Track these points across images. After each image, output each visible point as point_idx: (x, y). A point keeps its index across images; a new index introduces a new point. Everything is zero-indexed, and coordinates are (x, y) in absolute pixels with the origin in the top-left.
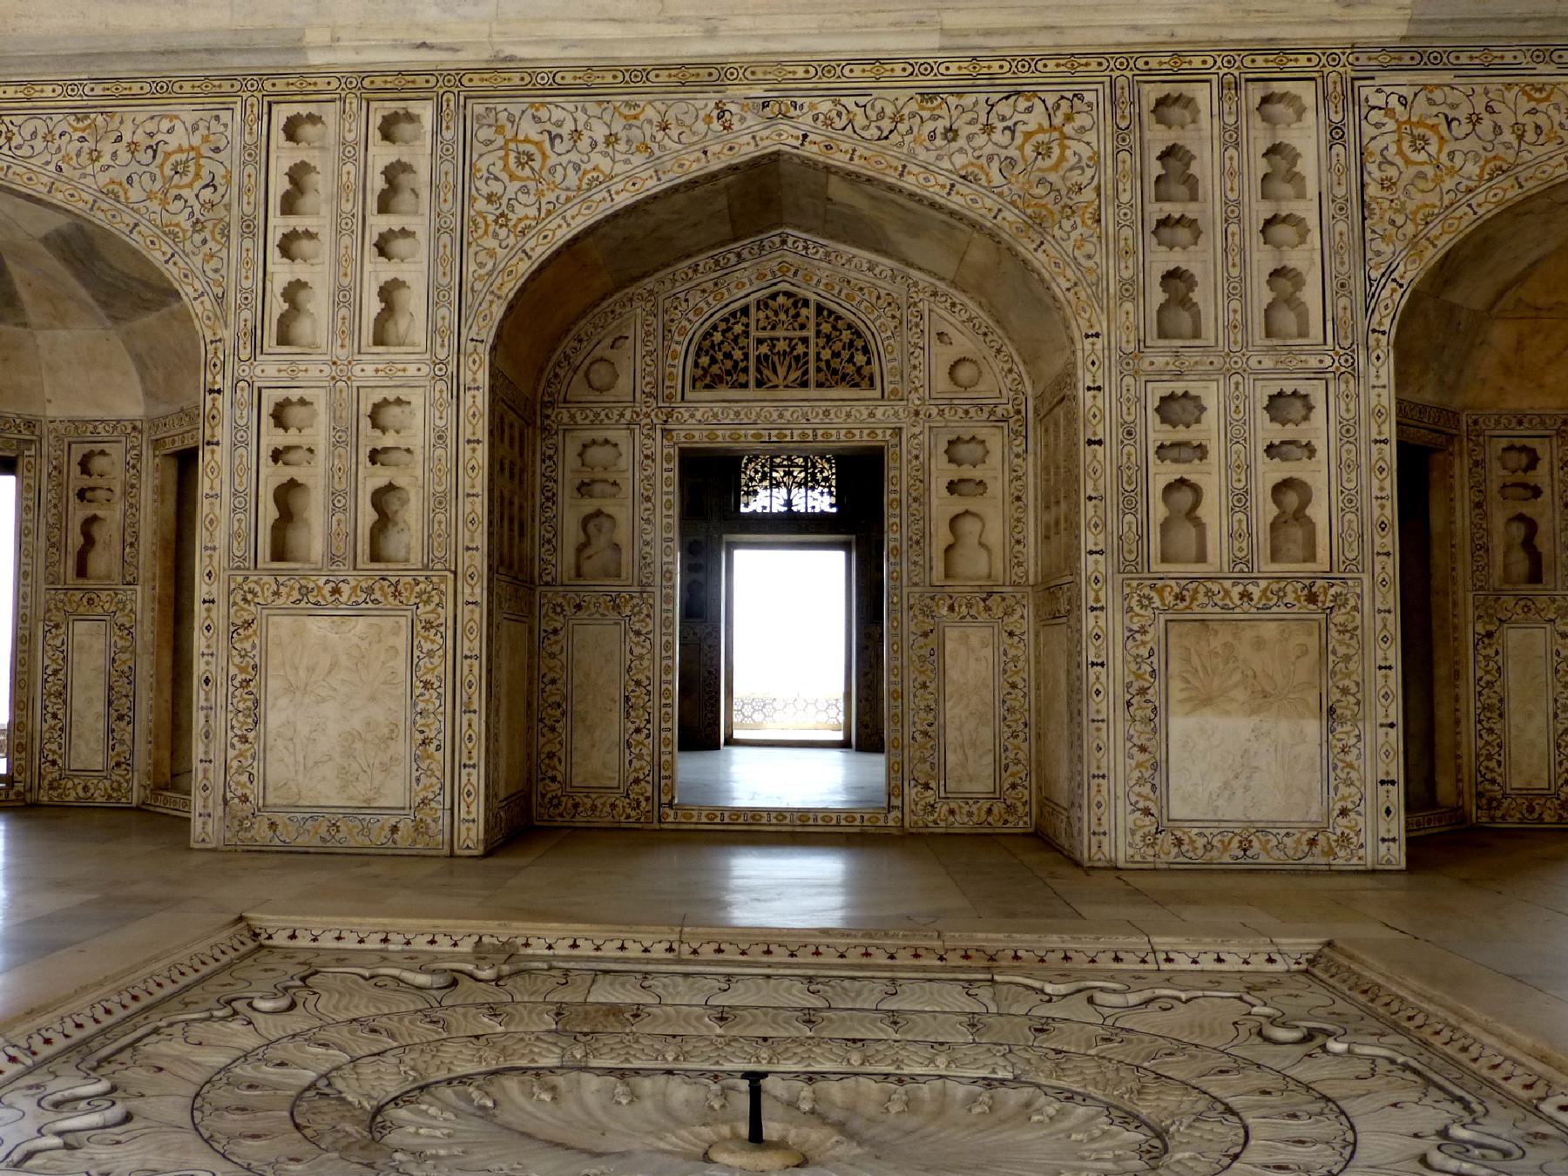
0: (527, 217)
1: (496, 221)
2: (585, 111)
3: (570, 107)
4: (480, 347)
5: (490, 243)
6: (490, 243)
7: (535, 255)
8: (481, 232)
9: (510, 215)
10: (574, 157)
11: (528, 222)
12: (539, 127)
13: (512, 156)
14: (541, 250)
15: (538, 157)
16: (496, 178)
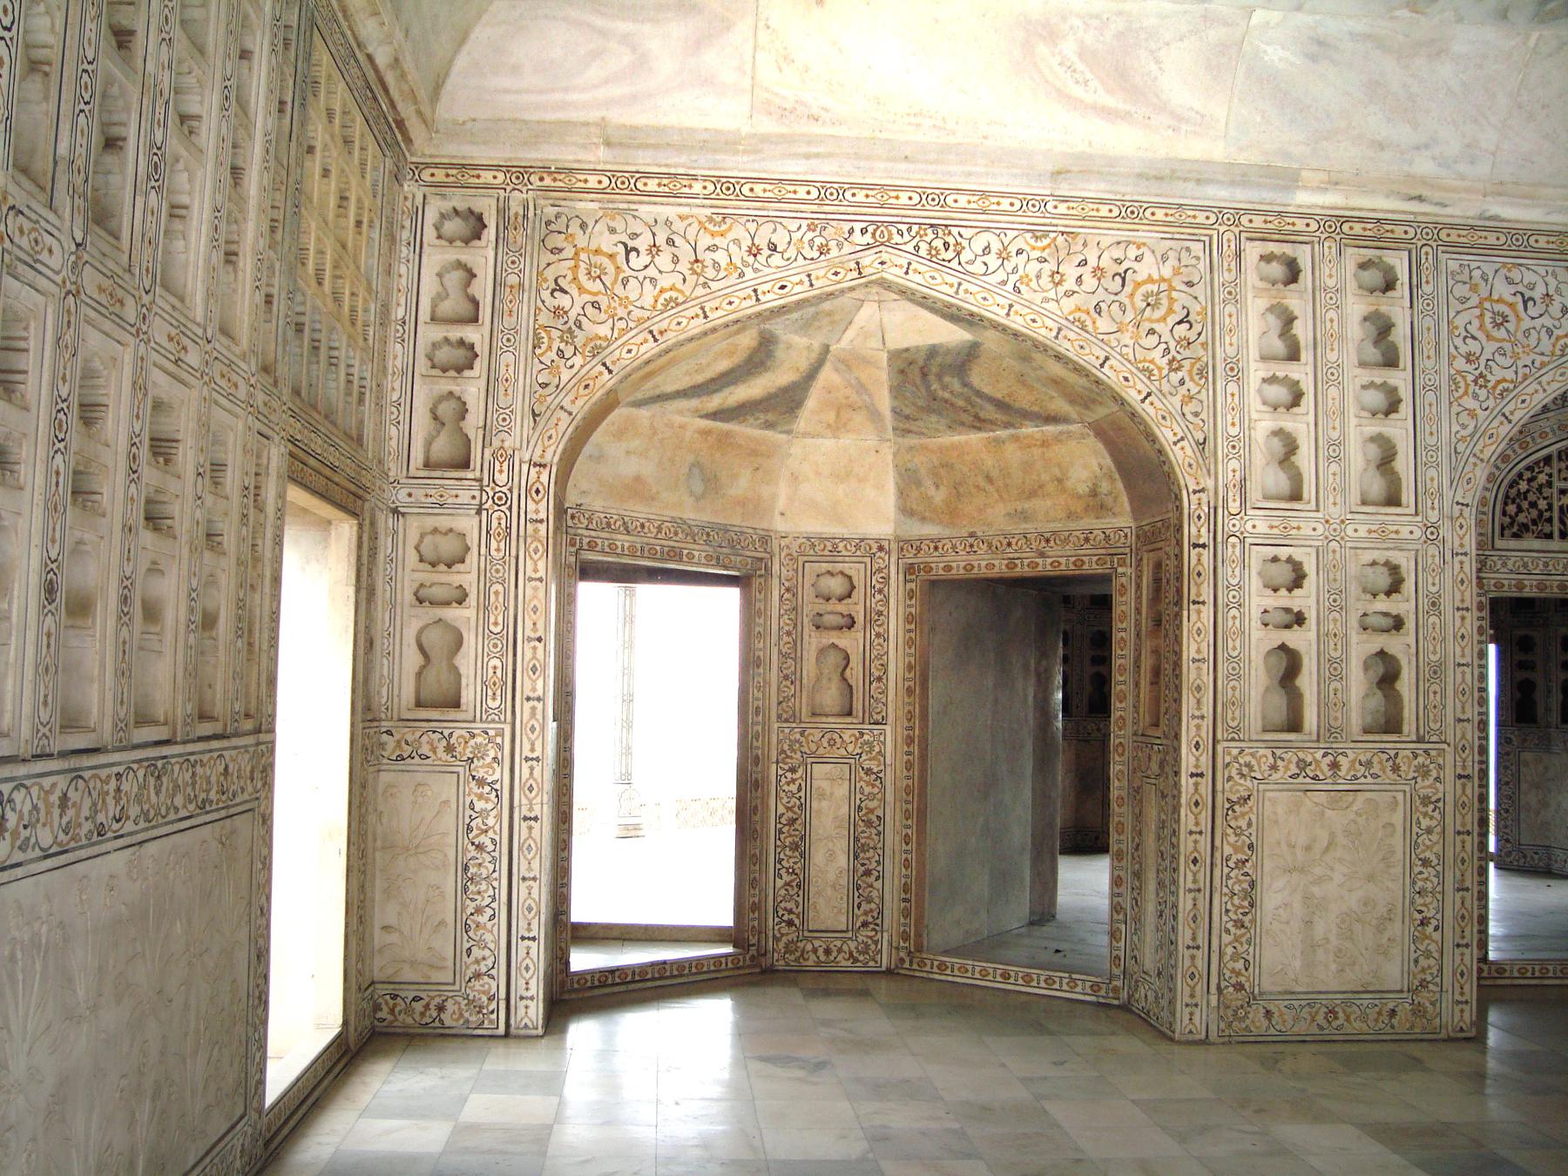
0: (1505, 380)
1: (1475, 382)
2: (1555, 275)
3: (1542, 271)
4: (1466, 511)
5: (1469, 402)
6: (1469, 402)
7: (1515, 419)
8: (1461, 391)
9: (1489, 377)
10: (1546, 321)
11: (1506, 385)
12: (1512, 289)
13: (1488, 315)
14: (1520, 415)
15: (1512, 318)
16: (1474, 338)
